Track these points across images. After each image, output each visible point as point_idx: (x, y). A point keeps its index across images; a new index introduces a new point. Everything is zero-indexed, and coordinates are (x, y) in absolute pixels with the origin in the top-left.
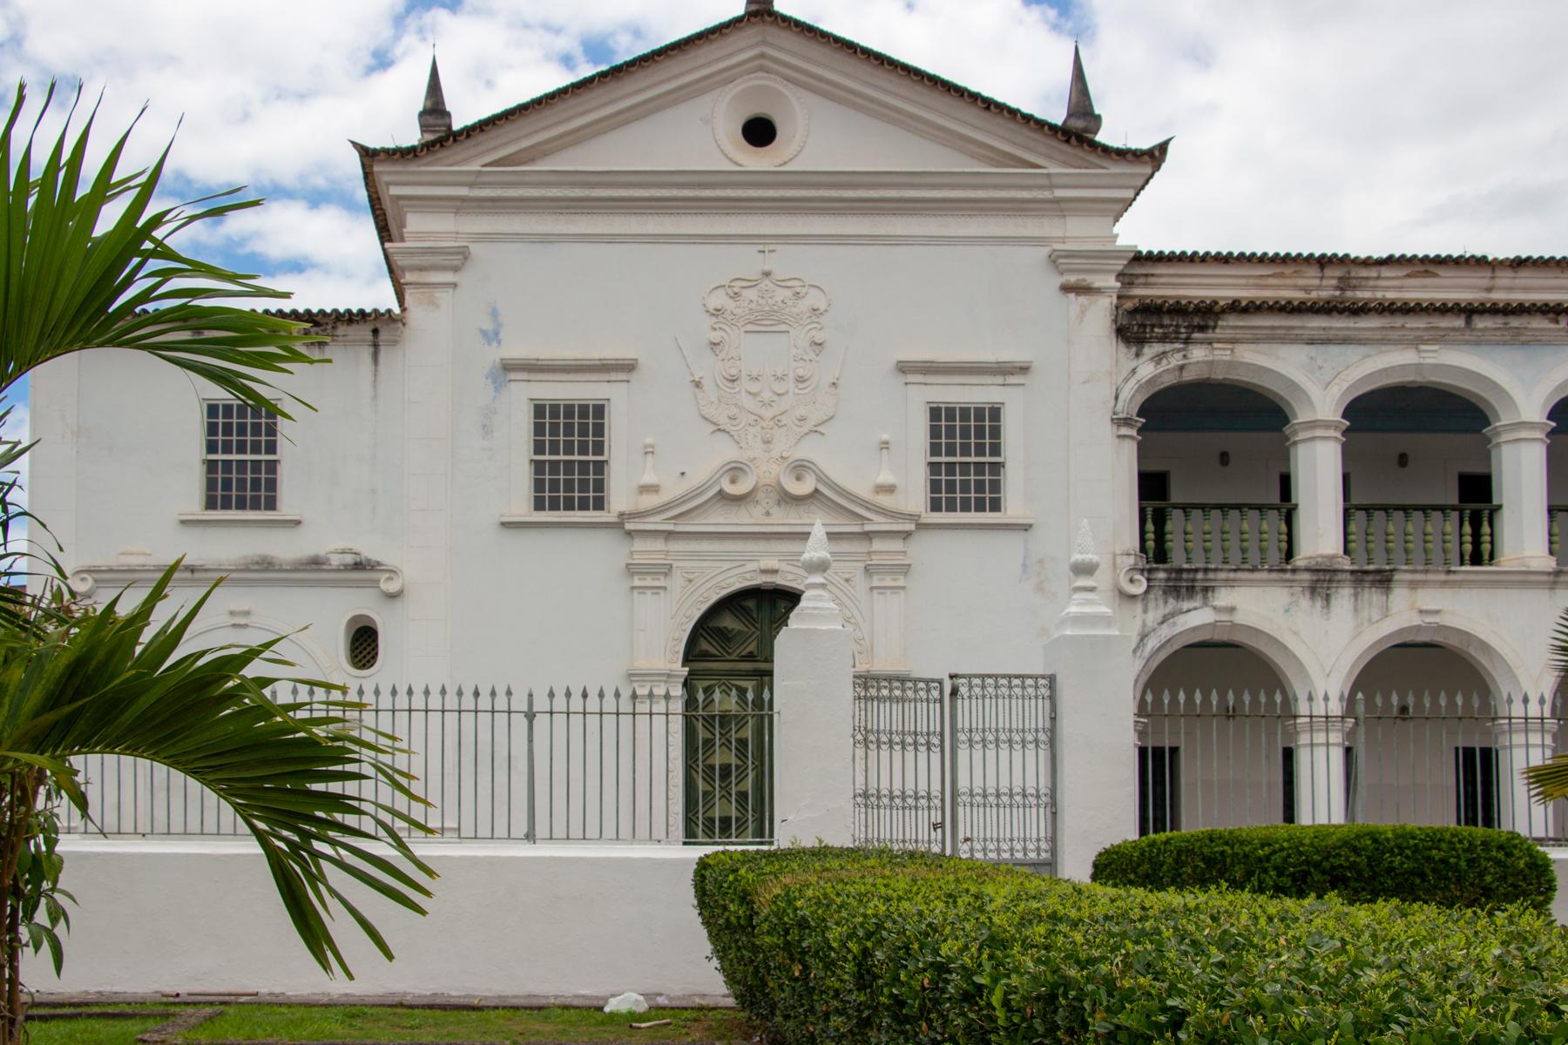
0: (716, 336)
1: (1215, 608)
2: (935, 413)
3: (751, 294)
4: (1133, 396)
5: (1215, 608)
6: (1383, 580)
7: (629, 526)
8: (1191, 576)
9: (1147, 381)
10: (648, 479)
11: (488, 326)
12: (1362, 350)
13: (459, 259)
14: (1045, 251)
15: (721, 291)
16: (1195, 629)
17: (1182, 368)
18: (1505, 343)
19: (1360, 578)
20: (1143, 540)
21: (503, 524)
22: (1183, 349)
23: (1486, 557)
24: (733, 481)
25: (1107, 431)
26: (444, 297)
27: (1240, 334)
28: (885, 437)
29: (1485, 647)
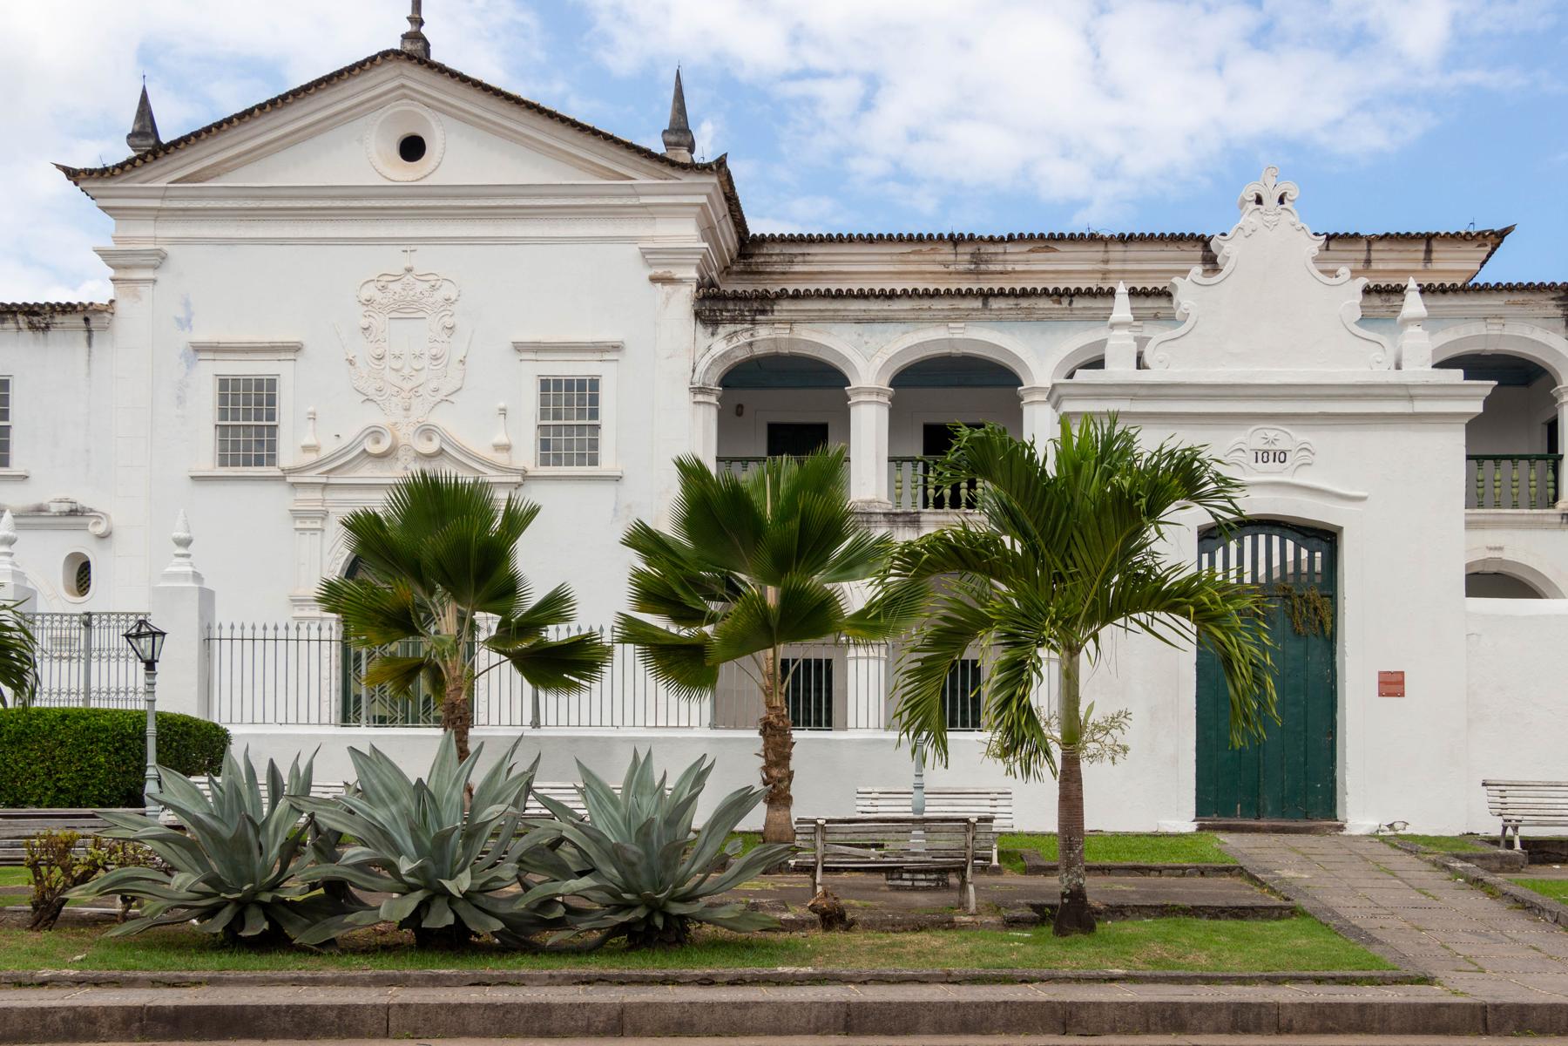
0: (365, 322)
3: (396, 287)
4: (708, 369)
7: (290, 480)
9: (721, 356)
10: (309, 440)
11: (182, 315)
12: (902, 327)
13: (158, 260)
15: (371, 284)
17: (751, 344)
18: (1022, 320)
22: (751, 329)
24: (378, 442)
26: (145, 290)
28: (502, 405)
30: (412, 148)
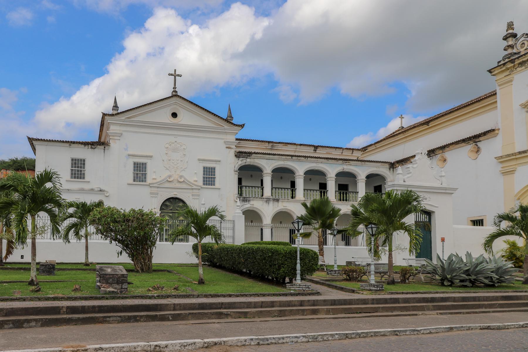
1: (250, 204)
2: (204, 168)
5: (250, 204)
6: (278, 200)
8: (247, 198)
14: (223, 141)
16: (247, 208)
17: (246, 162)
19: (274, 200)
20: (238, 192)
21: (128, 184)
23: (294, 197)
25: (233, 173)
27: (255, 157)
28: (196, 172)
29: (293, 212)
30: (174, 115)
